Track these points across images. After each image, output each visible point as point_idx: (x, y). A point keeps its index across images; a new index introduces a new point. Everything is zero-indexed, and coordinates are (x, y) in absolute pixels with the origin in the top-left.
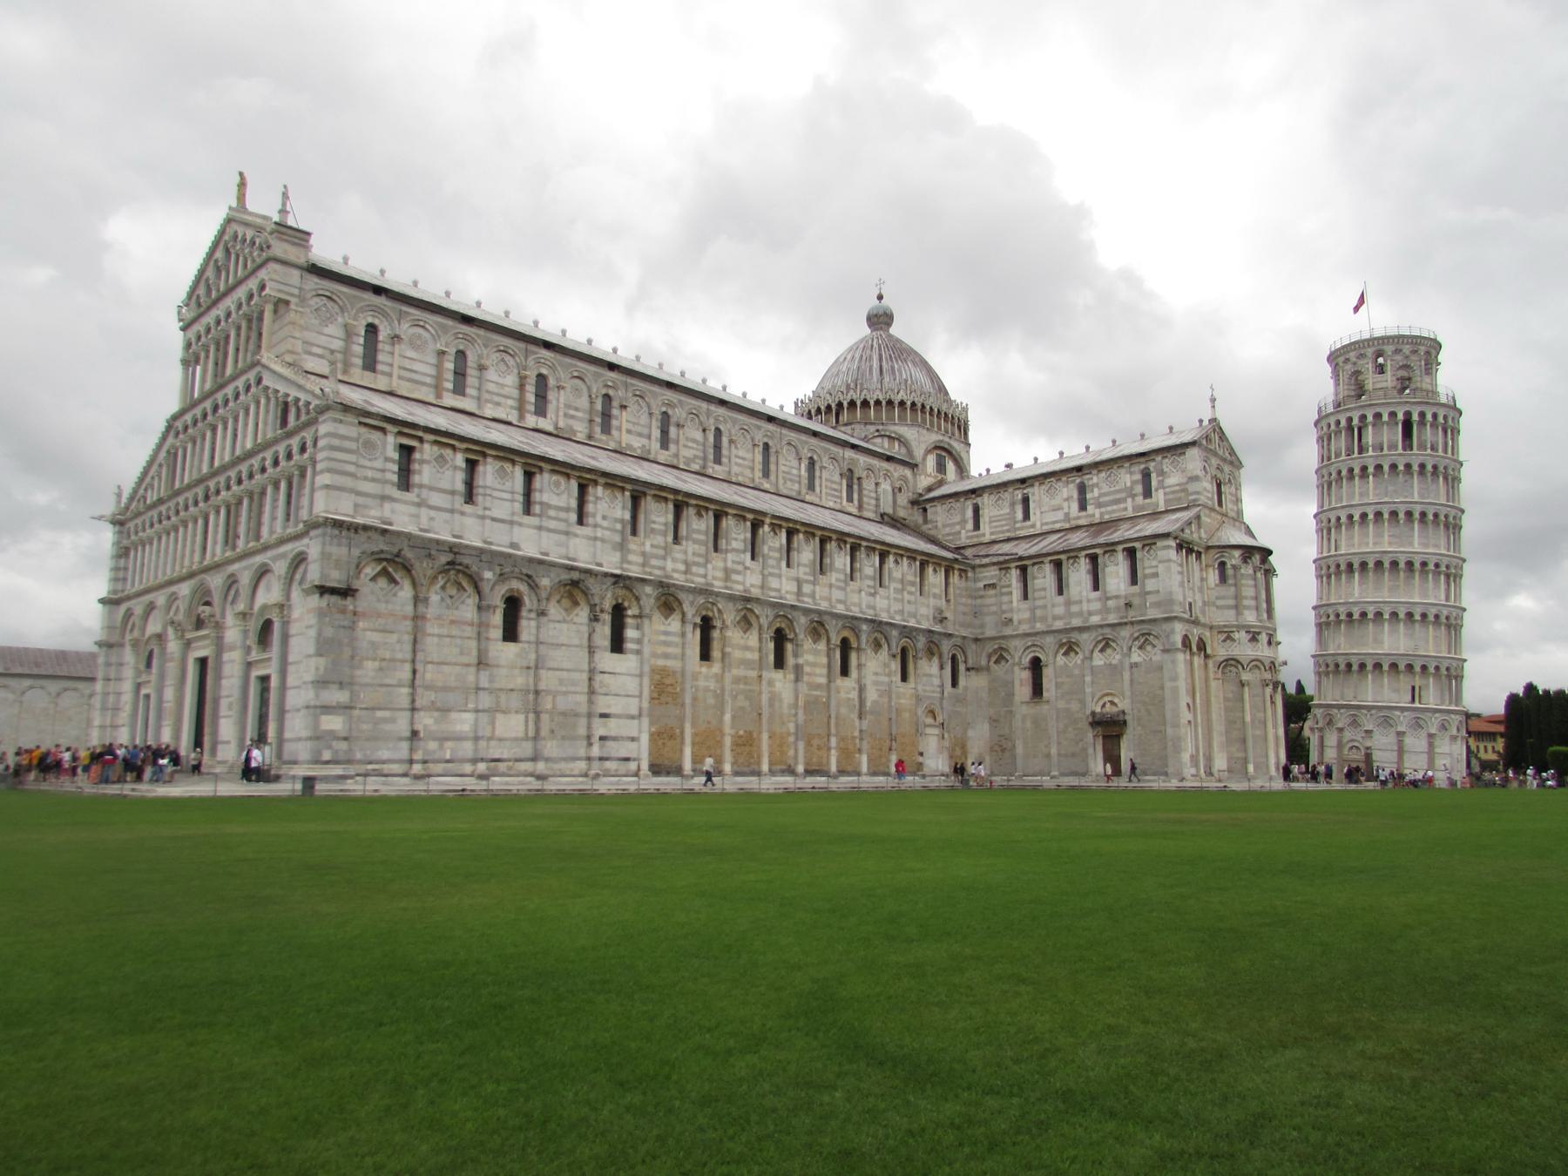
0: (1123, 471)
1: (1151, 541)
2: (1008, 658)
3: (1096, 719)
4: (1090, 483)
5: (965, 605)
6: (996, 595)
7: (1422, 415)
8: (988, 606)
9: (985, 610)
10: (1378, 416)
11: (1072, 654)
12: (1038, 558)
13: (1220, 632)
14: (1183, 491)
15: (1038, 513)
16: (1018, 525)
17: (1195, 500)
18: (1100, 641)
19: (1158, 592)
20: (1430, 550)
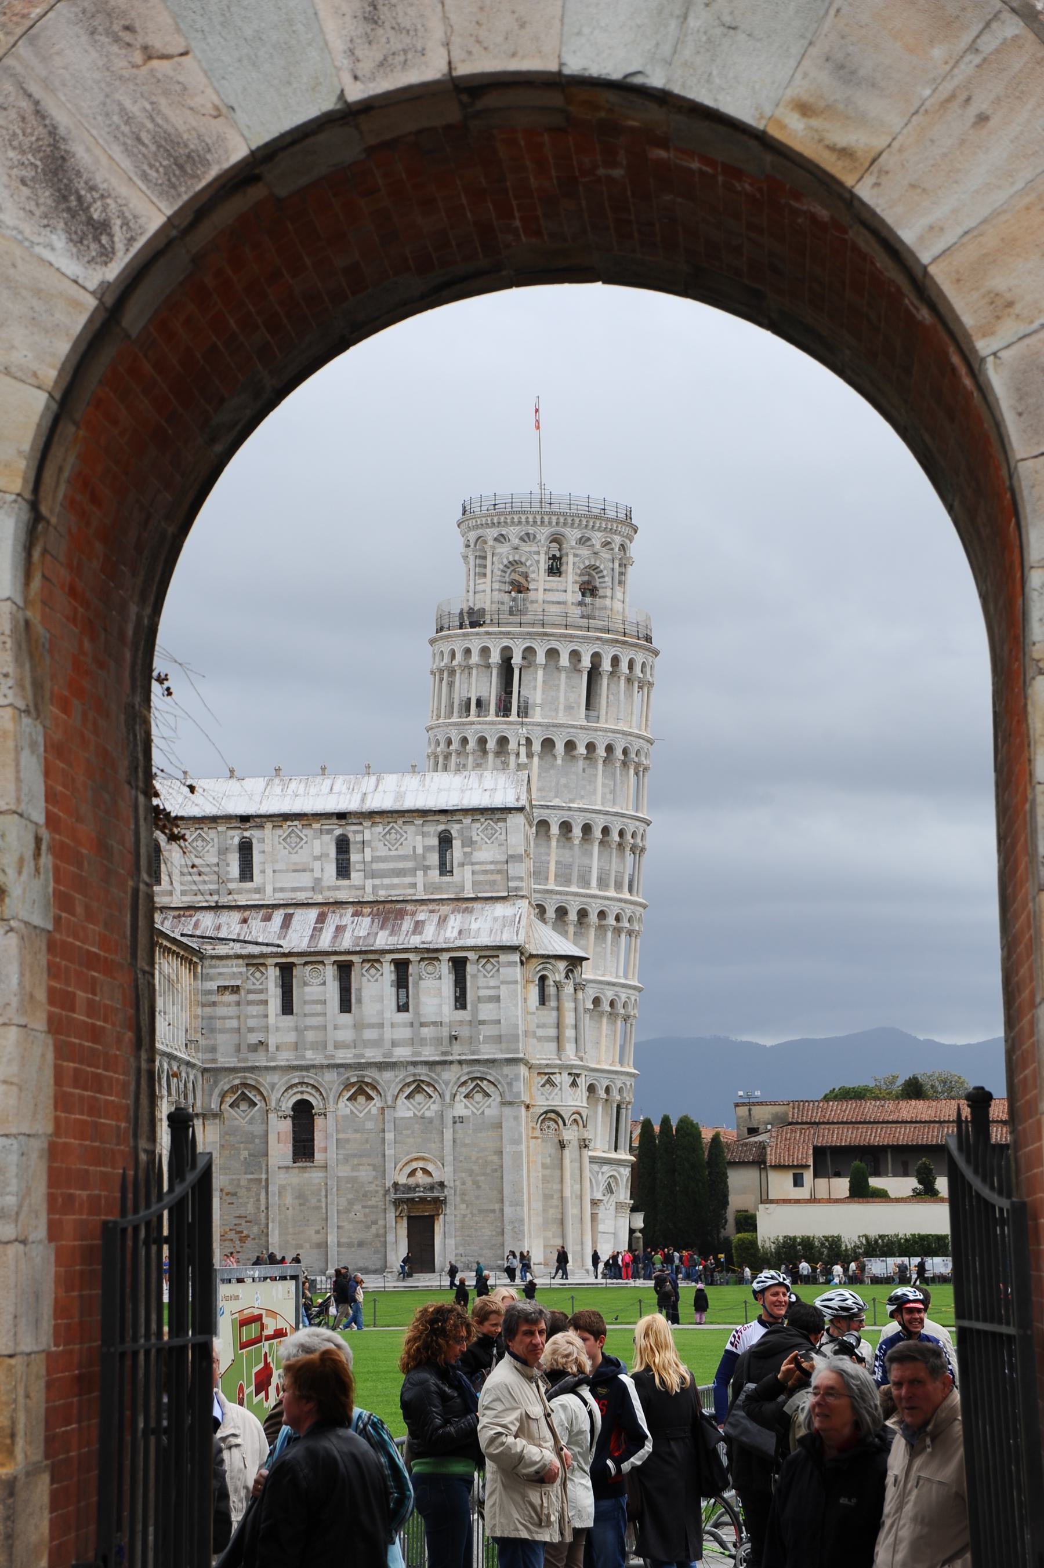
0: (410, 829)
1: (491, 953)
2: (257, 1099)
3: (399, 1196)
4: (359, 838)
5: (196, 1017)
6: (238, 1004)
7: (615, 661)
8: (224, 1018)
9: (218, 1024)
10: (552, 654)
11: (361, 1099)
12: (314, 957)
13: (539, 1073)
14: (499, 872)
15: (269, 871)
16: (232, 886)
17: (517, 889)
18: (408, 1084)
19: (499, 1022)
20: (611, 893)
